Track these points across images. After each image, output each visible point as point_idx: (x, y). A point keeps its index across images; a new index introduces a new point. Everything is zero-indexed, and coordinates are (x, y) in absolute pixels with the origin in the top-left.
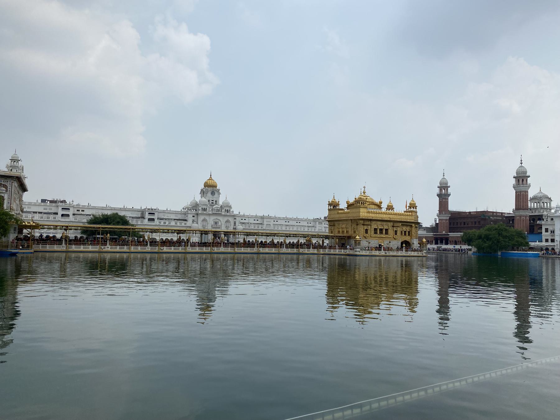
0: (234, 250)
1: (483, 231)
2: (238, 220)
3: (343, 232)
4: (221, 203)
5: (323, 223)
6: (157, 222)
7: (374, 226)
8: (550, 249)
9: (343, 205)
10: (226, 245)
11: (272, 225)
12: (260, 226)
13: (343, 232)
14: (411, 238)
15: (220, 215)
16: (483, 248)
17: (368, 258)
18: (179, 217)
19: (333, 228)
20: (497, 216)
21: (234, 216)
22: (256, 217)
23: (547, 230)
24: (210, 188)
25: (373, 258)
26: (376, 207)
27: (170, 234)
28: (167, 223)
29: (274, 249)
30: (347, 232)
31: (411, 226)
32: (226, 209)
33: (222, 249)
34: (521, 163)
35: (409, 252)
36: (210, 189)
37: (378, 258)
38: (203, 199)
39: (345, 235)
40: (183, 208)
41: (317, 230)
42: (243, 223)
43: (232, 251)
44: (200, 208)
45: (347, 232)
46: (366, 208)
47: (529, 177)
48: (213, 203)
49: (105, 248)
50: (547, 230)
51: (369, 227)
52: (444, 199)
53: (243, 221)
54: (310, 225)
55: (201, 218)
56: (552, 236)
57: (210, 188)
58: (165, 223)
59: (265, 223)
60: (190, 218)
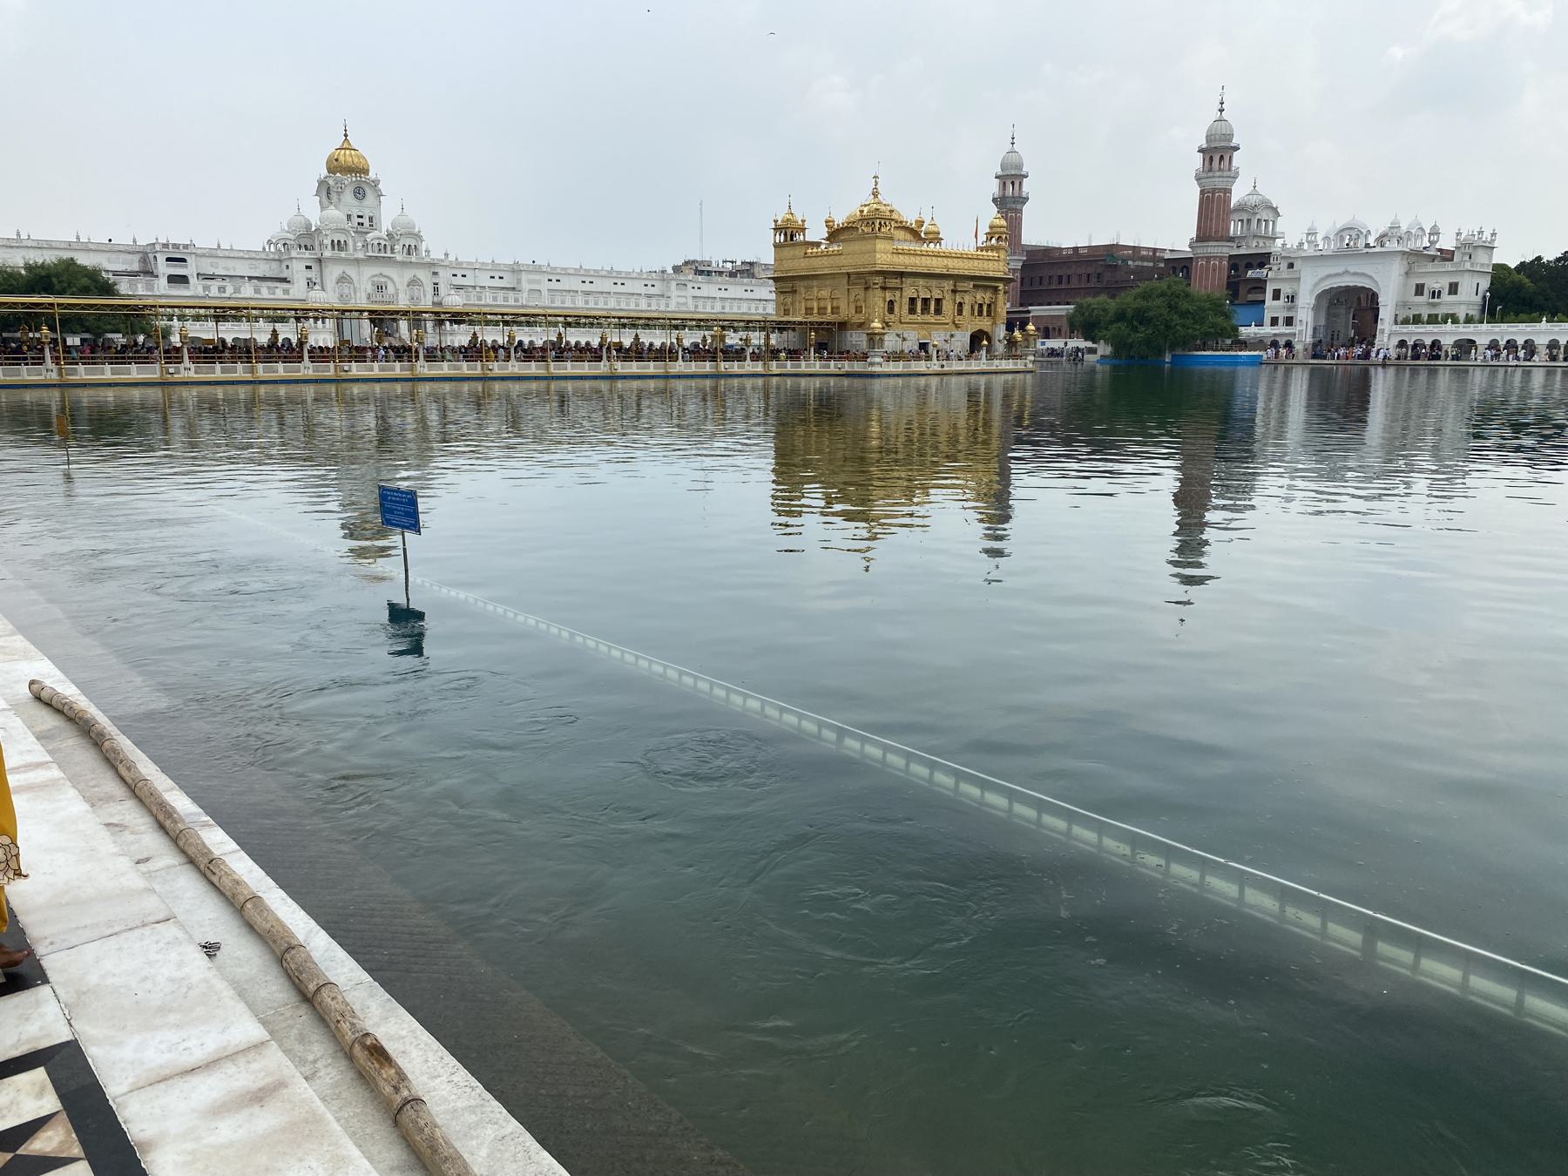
1: (1128, 299)
2: (444, 276)
3: (822, 311)
4: (386, 225)
5: (690, 285)
6: (196, 288)
7: (910, 292)
8: (1282, 342)
9: (816, 232)
10: (432, 355)
11: (545, 293)
12: (511, 294)
13: (822, 311)
14: (994, 323)
16: (1131, 346)
17: (900, 381)
18: (263, 269)
19: (789, 300)
20: (1143, 259)
22: (495, 270)
24: (347, 175)
25: (913, 380)
26: (909, 236)
27: (244, 326)
28: (229, 290)
29: (652, 364)
30: (835, 310)
31: (996, 289)
32: (402, 247)
34: (1221, 111)
35: (996, 362)
36: (348, 179)
37: (922, 381)
39: (829, 317)
40: (270, 242)
41: (672, 308)
42: (459, 288)
43: (542, 372)
44: (327, 242)
45: (835, 310)
46: (891, 239)
47: (1236, 148)
48: (364, 224)
51: (898, 293)
52: (1011, 210)
53: (459, 281)
54: (651, 291)
55: (333, 272)
56: (1289, 309)
57: (347, 175)
58: (222, 289)
59: (525, 286)
60: (298, 272)
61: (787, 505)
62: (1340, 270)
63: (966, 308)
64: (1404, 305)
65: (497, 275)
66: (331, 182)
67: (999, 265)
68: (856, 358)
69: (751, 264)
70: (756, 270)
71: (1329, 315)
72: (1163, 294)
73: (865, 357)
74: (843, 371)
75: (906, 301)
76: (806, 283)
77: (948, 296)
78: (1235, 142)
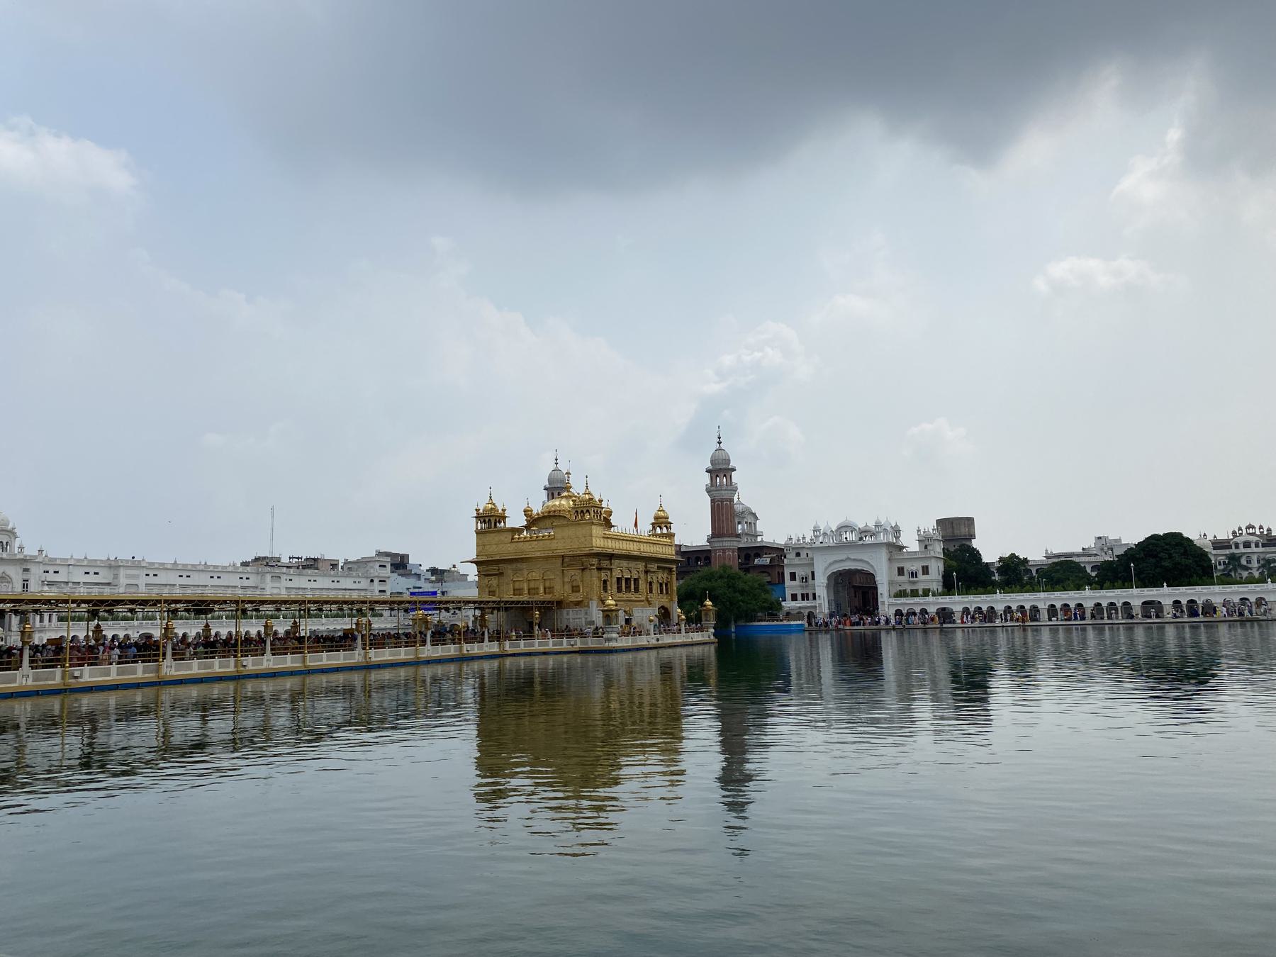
2: (36, 571)
5: (284, 577)
7: (617, 573)
9: (516, 520)
17: (630, 656)
19: (494, 581)
21: (25, 561)
22: (90, 566)
23: (793, 576)
31: (670, 570)
33: (269, 662)
43: (297, 665)
47: (734, 470)
50: (793, 576)
53: (51, 577)
54: (246, 583)
59: (123, 581)
62: (844, 557)
63: (655, 586)
64: (891, 583)
65: (92, 571)
67: (670, 553)
69: (315, 560)
70: (320, 565)
71: (836, 593)
72: (721, 577)
74: (577, 647)
75: (614, 580)
76: (514, 565)
77: (642, 576)
78: (732, 464)
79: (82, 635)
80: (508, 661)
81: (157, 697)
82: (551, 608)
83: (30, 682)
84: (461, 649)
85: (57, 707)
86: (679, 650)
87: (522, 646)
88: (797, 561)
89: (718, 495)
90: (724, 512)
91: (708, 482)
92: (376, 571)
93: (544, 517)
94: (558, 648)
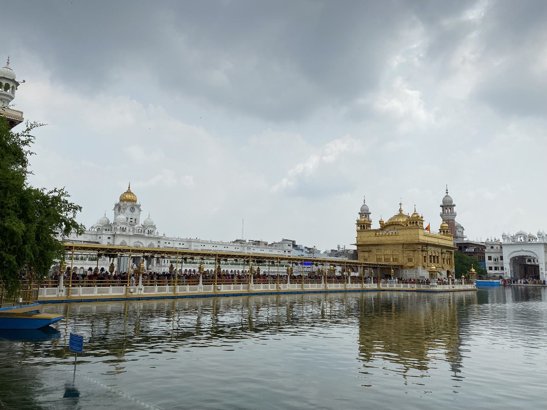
0: (302, 287)
2: (162, 242)
4: (141, 222)
5: (252, 248)
7: (430, 253)
9: (375, 226)
13: (388, 260)
15: (143, 237)
21: (159, 238)
23: (490, 258)
24: (128, 202)
27: (80, 262)
31: (451, 253)
32: (148, 230)
34: (447, 193)
36: (129, 204)
38: (122, 217)
39: (392, 263)
40: (92, 227)
44: (119, 228)
45: (395, 260)
47: (454, 206)
48: (133, 222)
49: (135, 291)
50: (490, 258)
54: (237, 250)
56: (496, 264)
57: (128, 202)
61: (366, 351)
62: (520, 249)
63: (445, 261)
66: (121, 205)
68: (423, 283)
69: (259, 242)
70: (261, 244)
71: (514, 267)
73: (428, 282)
75: (429, 257)
76: (377, 247)
77: (440, 255)
79: (214, 270)
80: (381, 293)
81: (248, 301)
82: (399, 268)
83: (202, 291)
84: (362, 286)
85: (212, 301)
86: (462, 293)
87: (388, 286)
88: (492, 250)
89: (446, 218)
90: (450, 227)
91: (441, 211)
92: (286, 247)
93: (390, 225)
94: (405, 288)
